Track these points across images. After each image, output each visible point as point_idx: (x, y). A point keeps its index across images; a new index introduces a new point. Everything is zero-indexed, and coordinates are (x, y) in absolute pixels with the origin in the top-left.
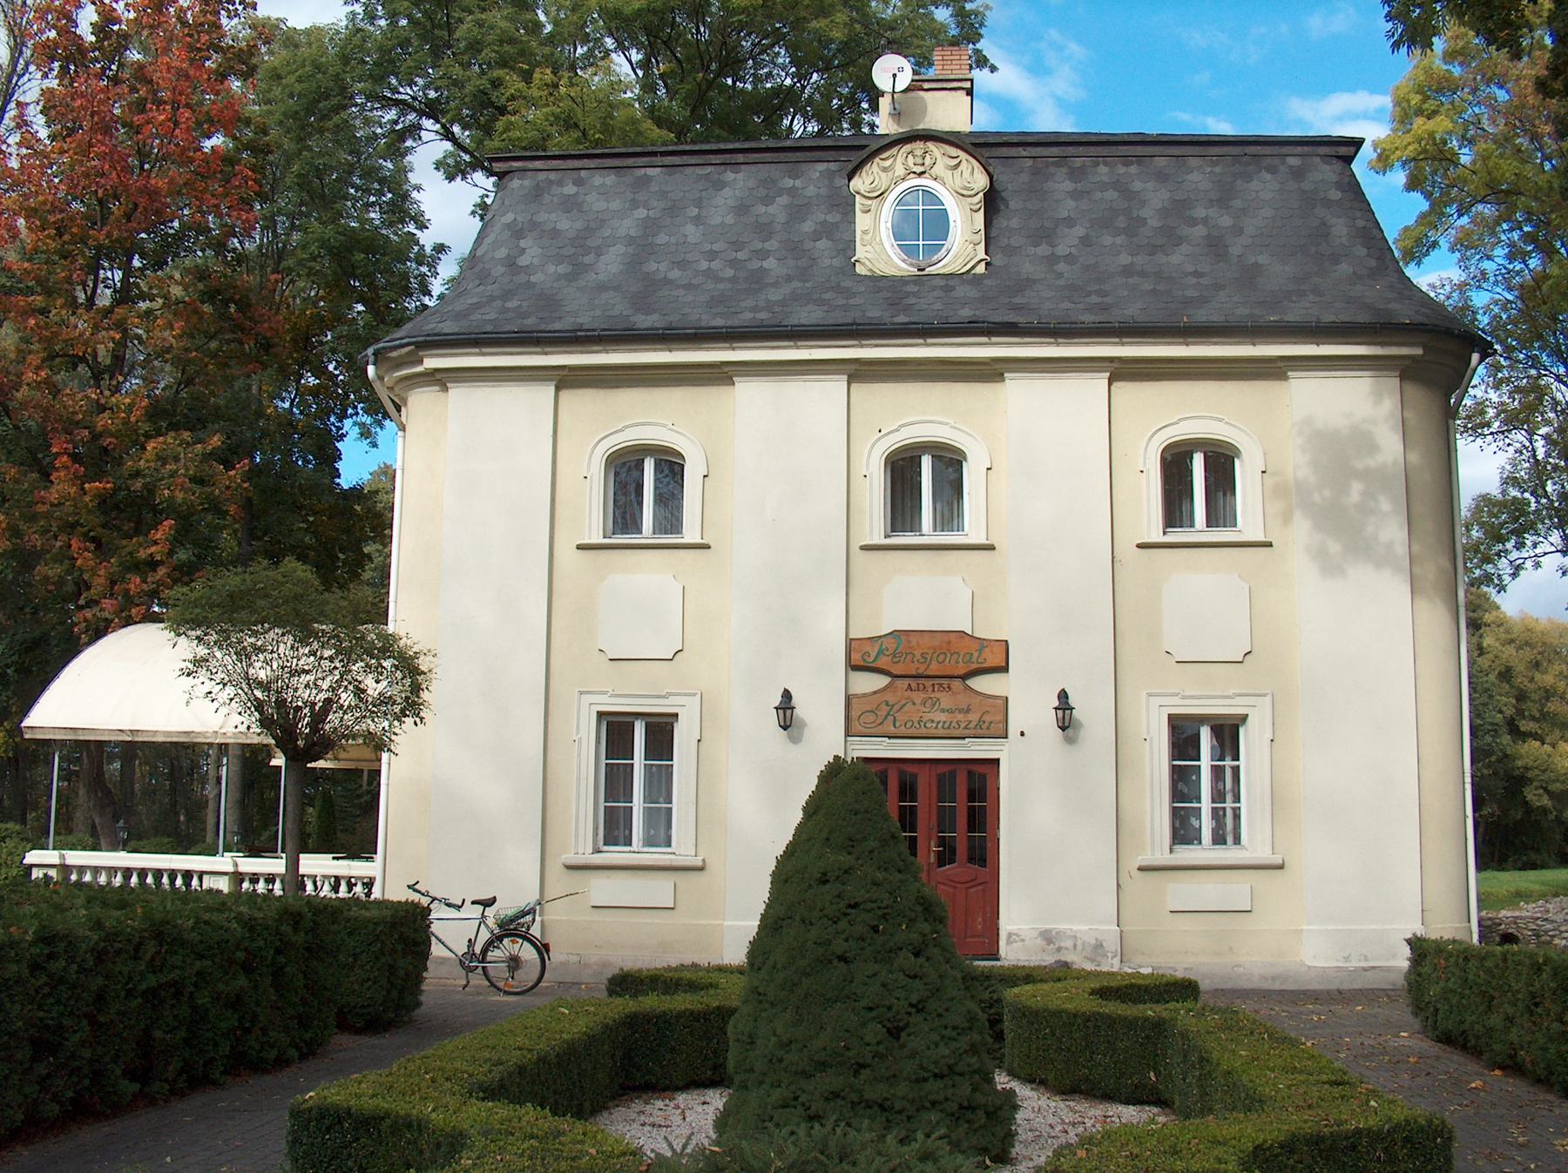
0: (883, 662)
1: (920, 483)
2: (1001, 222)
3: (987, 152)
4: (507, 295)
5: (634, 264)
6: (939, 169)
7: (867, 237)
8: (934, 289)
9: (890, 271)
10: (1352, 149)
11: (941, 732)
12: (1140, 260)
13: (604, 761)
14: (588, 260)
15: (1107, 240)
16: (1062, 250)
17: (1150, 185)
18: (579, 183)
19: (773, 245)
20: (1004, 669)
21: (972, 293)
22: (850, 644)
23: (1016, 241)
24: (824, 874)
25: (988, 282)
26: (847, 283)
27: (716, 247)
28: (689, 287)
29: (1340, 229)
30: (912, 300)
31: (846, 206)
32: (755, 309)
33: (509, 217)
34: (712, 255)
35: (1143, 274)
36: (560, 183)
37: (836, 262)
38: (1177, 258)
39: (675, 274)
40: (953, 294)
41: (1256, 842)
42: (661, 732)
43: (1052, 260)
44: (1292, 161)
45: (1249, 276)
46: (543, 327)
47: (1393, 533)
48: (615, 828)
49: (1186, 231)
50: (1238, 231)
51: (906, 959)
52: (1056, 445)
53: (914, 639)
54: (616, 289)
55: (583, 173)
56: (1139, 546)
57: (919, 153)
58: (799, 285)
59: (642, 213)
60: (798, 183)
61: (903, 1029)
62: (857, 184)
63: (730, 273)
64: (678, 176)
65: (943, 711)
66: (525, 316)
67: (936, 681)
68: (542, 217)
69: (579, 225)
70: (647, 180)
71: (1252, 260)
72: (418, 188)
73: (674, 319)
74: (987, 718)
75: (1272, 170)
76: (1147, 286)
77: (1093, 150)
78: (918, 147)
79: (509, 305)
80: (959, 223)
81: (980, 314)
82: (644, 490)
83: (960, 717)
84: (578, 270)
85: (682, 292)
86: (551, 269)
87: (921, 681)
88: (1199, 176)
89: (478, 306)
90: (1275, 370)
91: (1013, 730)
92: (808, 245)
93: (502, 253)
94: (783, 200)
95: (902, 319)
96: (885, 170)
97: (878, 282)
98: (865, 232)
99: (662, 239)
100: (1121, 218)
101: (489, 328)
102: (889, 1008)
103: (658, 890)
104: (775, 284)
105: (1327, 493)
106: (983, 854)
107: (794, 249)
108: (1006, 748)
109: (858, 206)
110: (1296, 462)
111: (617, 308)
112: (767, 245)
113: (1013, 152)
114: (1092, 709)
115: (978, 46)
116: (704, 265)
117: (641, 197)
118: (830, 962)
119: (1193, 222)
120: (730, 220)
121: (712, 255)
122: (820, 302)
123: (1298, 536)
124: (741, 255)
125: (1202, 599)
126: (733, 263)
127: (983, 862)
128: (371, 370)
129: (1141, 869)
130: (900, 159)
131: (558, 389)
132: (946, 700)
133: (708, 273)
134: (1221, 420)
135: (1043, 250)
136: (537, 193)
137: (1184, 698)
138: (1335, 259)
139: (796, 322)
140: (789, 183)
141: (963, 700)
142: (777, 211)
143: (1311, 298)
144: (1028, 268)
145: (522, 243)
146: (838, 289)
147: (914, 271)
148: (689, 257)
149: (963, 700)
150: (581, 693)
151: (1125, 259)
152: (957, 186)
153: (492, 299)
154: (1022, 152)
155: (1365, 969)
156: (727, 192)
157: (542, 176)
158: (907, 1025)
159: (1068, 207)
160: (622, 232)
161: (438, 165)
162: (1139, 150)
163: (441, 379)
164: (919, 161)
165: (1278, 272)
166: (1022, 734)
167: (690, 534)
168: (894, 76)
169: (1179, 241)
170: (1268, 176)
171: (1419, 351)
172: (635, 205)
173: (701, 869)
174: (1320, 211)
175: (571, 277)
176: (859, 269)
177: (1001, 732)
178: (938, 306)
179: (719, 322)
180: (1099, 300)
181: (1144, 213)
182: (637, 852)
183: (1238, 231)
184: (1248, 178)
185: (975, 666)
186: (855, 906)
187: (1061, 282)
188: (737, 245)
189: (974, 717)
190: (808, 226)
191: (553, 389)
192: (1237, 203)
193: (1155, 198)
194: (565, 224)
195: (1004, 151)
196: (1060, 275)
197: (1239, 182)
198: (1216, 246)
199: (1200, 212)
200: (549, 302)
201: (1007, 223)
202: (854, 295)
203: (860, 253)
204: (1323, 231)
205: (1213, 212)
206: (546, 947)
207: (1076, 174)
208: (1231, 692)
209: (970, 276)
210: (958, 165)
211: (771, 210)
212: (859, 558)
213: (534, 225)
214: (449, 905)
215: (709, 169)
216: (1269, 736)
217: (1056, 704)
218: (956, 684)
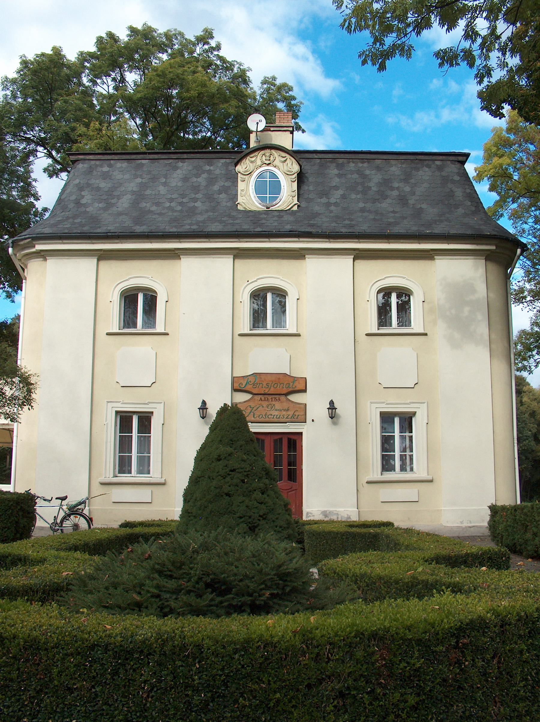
0: (248, 388)
1: (267, 306)
2: (305, 187)
3: (299, 156)
4: (75, 217)
5: (135, 204)
6: (277, 163)
7: (243, 193)
8: (274, 216)
9: (253, 208)
10: (465, 158)
11: (276, 420)
12: (368, 205)
13: (118, 434)
14: (113, 201)
15: (353, 196)
16: (332, 200)
17: (373, 172)
18: (110, 166)
19: (199, 196)
20: (305, 391)
21: (291, 219)
22: (234, 379)
23: (311, 196)
24: (219, 456)
25: (299, 214)
26: (234, 214)
27: (173, 196)
28: (160, 214)
29: (459, 193)
30: (264, 221)
31: (233, 178)
32: (190, 224)
33: (77, 181)
34: (171, 200)
35: (369, 211)
36: (101, 166)
37: (229, 204)
38: (385, 205)
39: (154, 208)
40: (283, 219)
41: (420, 470)
42: (145, 420)
43: (328, 204)
44: (438, 163)
45: (418, 213)
46: (92, 231)
47: (483, 329)
48: (124, 465)
49: (389, 193)
50: (414, 194)
51: (257, 495)
52: (329, 288)
53: (263, 377)
54: (126, 214)
55: (112, 162)
56: (367, 335)
57: (268, 154)
58: (211, 214)
59: (139, 180)
60: (212, 168)
61: (256, 527)
62: (239, 168)
63: (179, 208)
64: (156, 163)
65: (276, 410)
66: (84, 226)
67: (273, 396)
68: (92, 181)
69: (109, 185)
70: (143, 165)
71: (419, 206)
72: (35, 180)
73: (153, 228)
74: (297, 414)
75: (429, 166)
76: (371, 216)
77: (347, 156)
79: (76, 221)
80: (285, 187)
81: (295, 228)
82: (138, 307)
83: (284, 413)
84: (109, 206)
85: (157, 216)
86: (96, 205)
87: (266, 396)
88: (396, 169)
89: (60, 222)
90: (429, 255)
91: (309, 419)
92: (216, 196)
93: (73, 197)
94: (205, 176)
96: (252, 162)
97: (247, 213)
98: (242, 190)
99: (148, 192)
100: (360, 186)
101: (66, 231)
102: (250, 517)
103: (144, 494)
104: (201, 213)
105: (453, 311)
106: (294, 474)
107: (209, 198)
108: (305, 427)
109: (239, 178)
110: (438, 295)
111: (127, 223)
112: (197, 196)
113: (311, 156)
114: (345, 409)
115: (297, 121)
116: (168, 204)
117: (139, 173)
118: (222, 496)
119: (392, 189)
120: (180, 184)
121: (171, 200)
122: (221, 222)
123: (439, 331)
124: (184, 200)
125: (395, 360)
126: (181, 204)
127: (295, 449)
128: (10, 250)
129: (368, 482)
130: (259, 157)
131: (98, 260)
132: (278, 405)
133: (170, 208)
134: (404, 278)
135: (324, 200)
136: (90, 171)
137: (387, 404)
138: (457, 206)
139: (210, 230)
140: (207, 168)
141: (286, 405)
142: (202, 180)
143: (446, 223)
144: (317, 208)
145: (83, 193)
146: (229, 216)
147: (265, 209)
148: (161, 201)
149: (286, 405)
150: (108, 402)
151: (361, 205)
153: (68, 218)
154: (315, 156)
155: (470, 527)
156: (179, 171)
157: (93, 162)
158: (258, 525)
159: (336, 181)
160: (130, 189)
161: (45, 170)
162: (369, 156)
163: (43, 255)
164: (268, 158)
165: (431, 212)
166: (313, 421)
167: (160, 328)
168: (257, 123)
169: (384, 197)
170: (427, 169)
171: (494, 248)
172: (136, 176)
173: (164, 484)
174: (450, 185)
175: (105, 209)
176: (239, 207)
177: (302, 420)
178: (276, 224)
179: (174, 230)
180: (349, 222)
181: (371, 184)
182: (134, 476)
183: (414, 194)
184: (418, 169)
185: (291, 389)
186: (233, 471)
187: (332, 215)
188: (183, 196)
189: (290, 413)
190: (216, 188)
191: (96, 260)
192: (413, 181)
193: (376, 178)
194: (104, 185)
195: (307, 155)
196: (331, 212)
197: (413, 171)
198: (403, 200)
199: (396, 185)
200: (95, 220)
201: (308, 187)
202: (237, 219)
203: (240, 200)
204: (451, 195)
205: (401, 185)
206: (91, 519)
207: (340, 167)
208: (408, 401)
209: (290, 211)
210: (286, 161)
211: (199, 180)
212: (237, 339)
213: (88, 185)
214: (45, 500)
215: (171, 161)
216: (426, 421)
217: (329, 406)
218: (283, 398)
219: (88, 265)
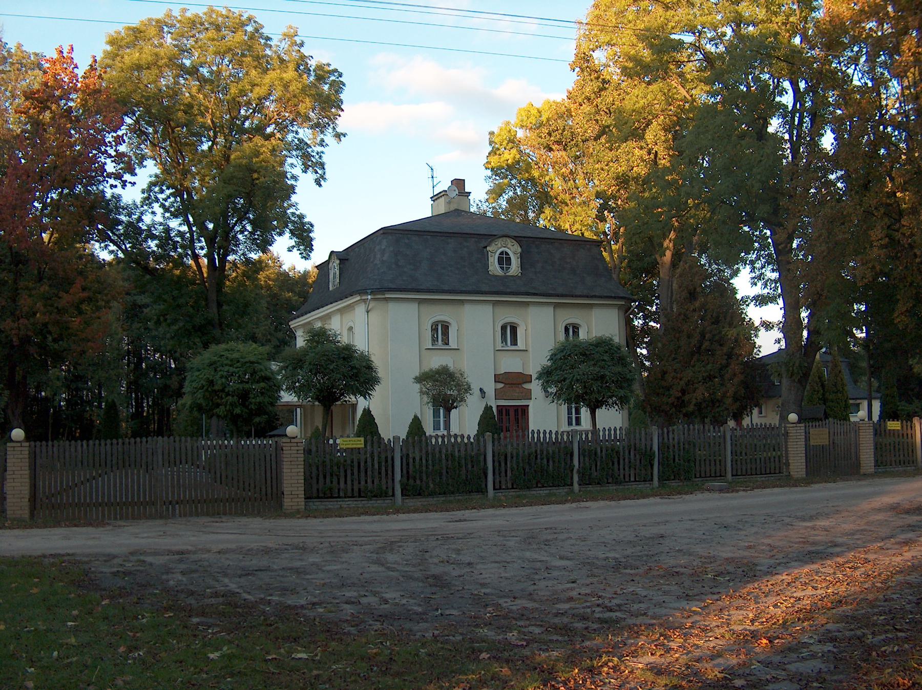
33: (392, 249)
78: (504, 239)
95: (508, 290)
132: (517, 390)
140: (465, 244)
152: (514, 251)
163: (386, 299)
199: (568, 260)
219: (414, 307)
